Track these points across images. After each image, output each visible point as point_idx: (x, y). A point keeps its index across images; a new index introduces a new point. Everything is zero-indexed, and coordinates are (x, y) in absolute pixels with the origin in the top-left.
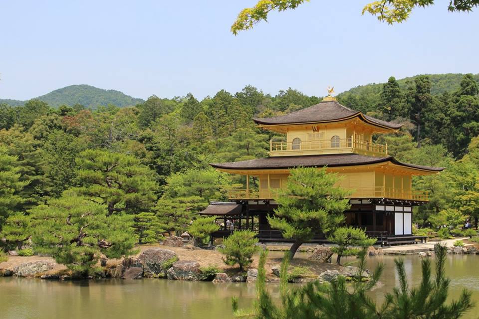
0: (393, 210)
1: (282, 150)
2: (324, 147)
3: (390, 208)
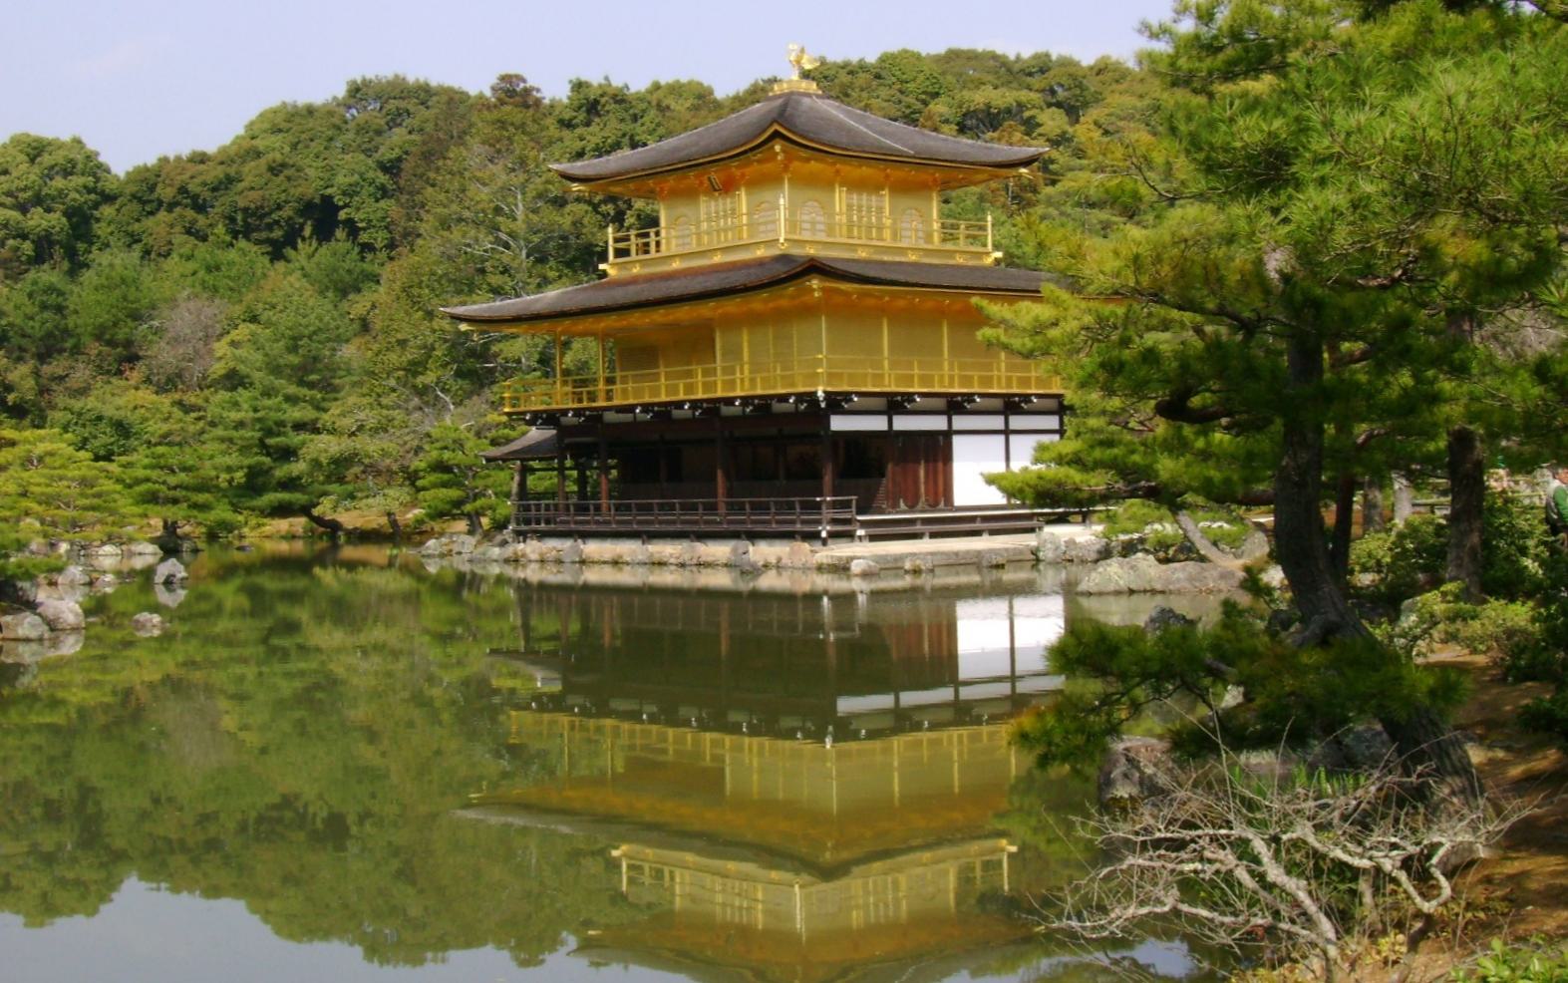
1: (634, 256)
3: (902, 423)
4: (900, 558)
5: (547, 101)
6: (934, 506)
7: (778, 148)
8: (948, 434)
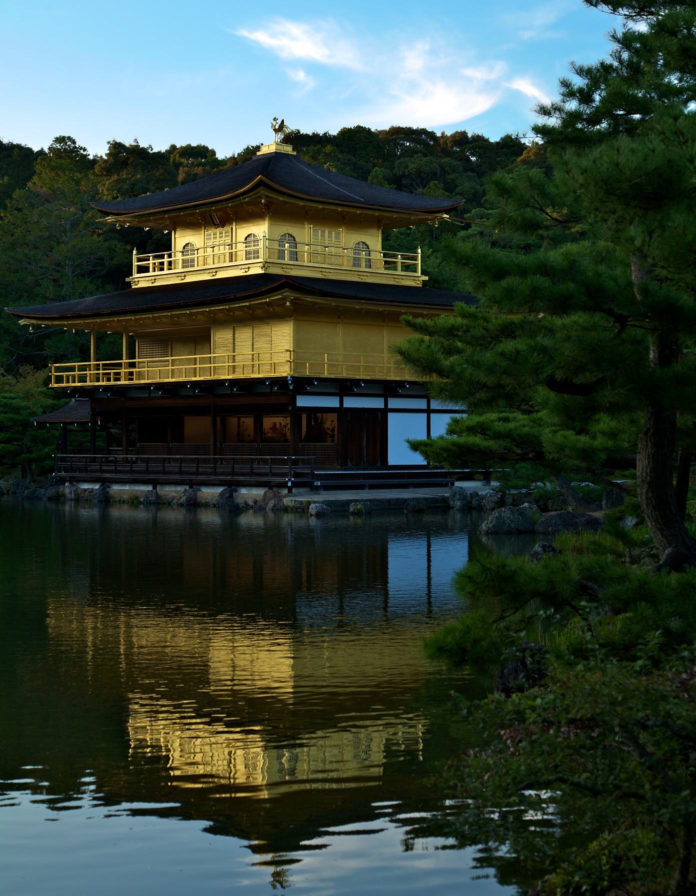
0: (382, 406)
3: (350, 403)
4: (348, 503)
5: (91, 157)
6: (372, 466)
8: (385, 411)
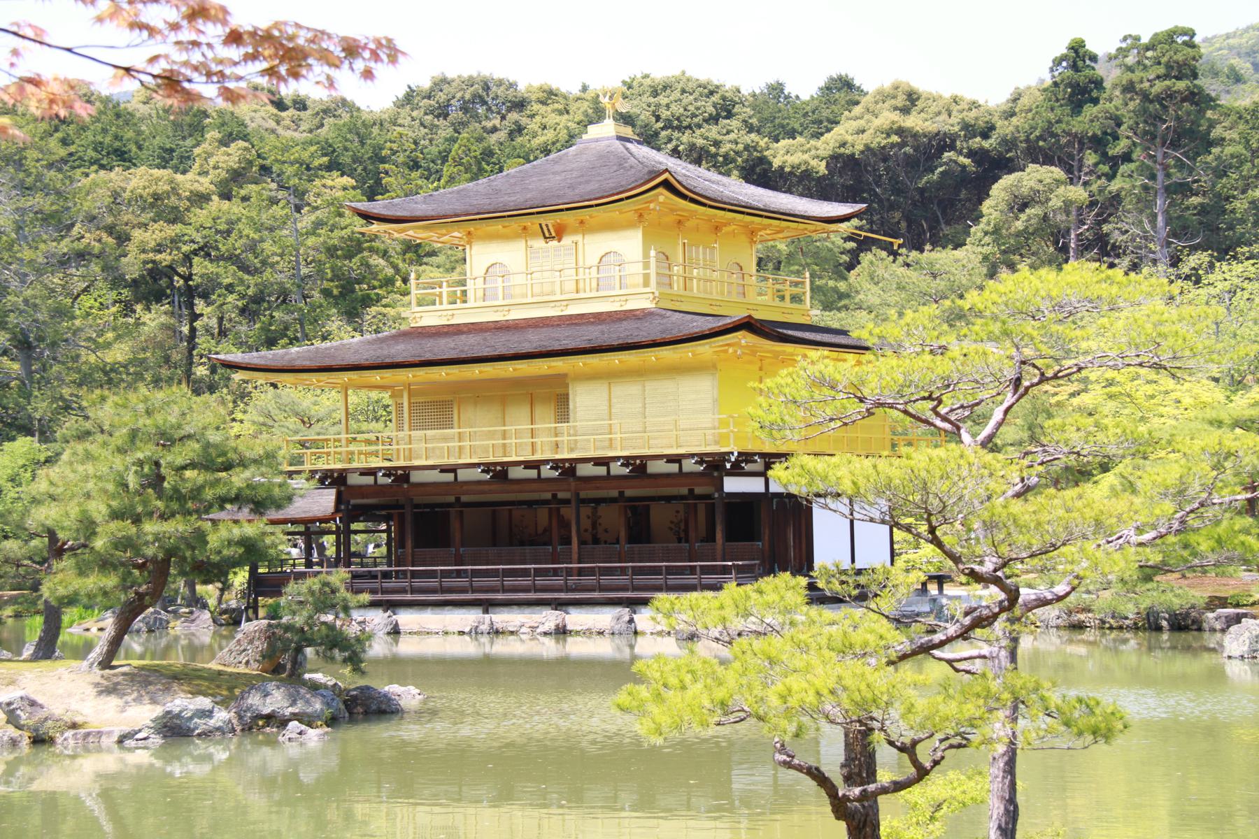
2: (511, 297)
7: (661, 199)
